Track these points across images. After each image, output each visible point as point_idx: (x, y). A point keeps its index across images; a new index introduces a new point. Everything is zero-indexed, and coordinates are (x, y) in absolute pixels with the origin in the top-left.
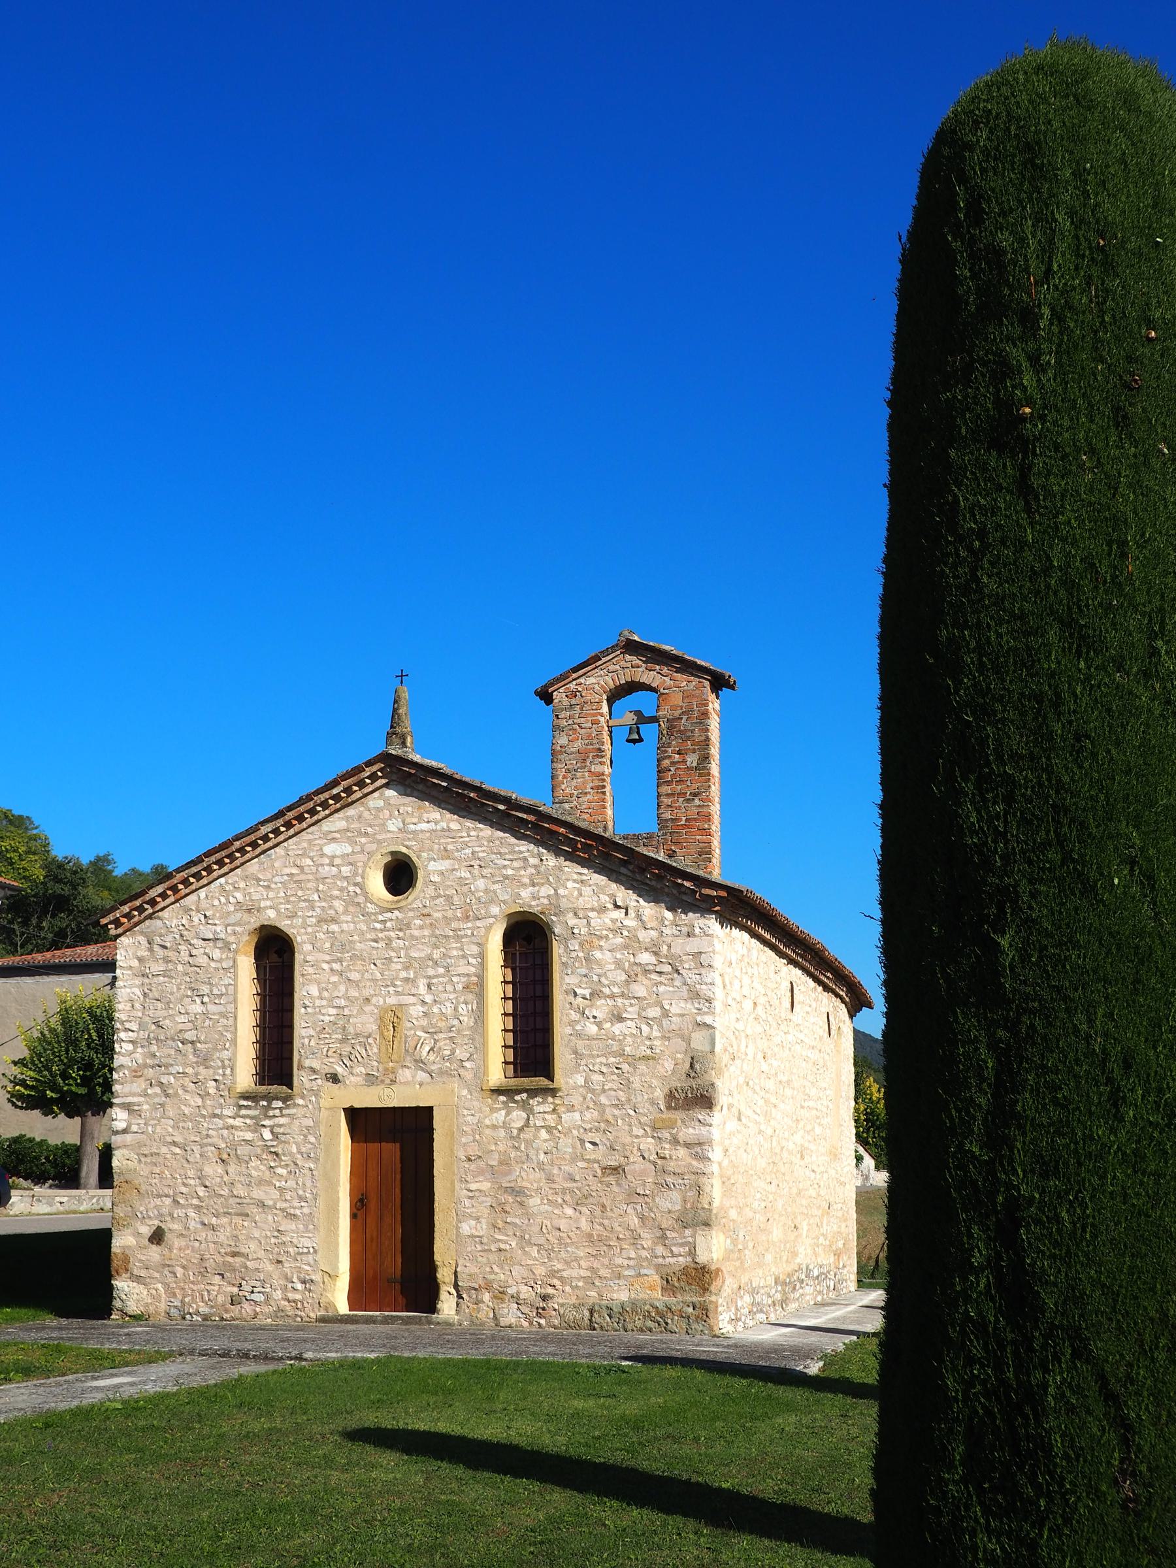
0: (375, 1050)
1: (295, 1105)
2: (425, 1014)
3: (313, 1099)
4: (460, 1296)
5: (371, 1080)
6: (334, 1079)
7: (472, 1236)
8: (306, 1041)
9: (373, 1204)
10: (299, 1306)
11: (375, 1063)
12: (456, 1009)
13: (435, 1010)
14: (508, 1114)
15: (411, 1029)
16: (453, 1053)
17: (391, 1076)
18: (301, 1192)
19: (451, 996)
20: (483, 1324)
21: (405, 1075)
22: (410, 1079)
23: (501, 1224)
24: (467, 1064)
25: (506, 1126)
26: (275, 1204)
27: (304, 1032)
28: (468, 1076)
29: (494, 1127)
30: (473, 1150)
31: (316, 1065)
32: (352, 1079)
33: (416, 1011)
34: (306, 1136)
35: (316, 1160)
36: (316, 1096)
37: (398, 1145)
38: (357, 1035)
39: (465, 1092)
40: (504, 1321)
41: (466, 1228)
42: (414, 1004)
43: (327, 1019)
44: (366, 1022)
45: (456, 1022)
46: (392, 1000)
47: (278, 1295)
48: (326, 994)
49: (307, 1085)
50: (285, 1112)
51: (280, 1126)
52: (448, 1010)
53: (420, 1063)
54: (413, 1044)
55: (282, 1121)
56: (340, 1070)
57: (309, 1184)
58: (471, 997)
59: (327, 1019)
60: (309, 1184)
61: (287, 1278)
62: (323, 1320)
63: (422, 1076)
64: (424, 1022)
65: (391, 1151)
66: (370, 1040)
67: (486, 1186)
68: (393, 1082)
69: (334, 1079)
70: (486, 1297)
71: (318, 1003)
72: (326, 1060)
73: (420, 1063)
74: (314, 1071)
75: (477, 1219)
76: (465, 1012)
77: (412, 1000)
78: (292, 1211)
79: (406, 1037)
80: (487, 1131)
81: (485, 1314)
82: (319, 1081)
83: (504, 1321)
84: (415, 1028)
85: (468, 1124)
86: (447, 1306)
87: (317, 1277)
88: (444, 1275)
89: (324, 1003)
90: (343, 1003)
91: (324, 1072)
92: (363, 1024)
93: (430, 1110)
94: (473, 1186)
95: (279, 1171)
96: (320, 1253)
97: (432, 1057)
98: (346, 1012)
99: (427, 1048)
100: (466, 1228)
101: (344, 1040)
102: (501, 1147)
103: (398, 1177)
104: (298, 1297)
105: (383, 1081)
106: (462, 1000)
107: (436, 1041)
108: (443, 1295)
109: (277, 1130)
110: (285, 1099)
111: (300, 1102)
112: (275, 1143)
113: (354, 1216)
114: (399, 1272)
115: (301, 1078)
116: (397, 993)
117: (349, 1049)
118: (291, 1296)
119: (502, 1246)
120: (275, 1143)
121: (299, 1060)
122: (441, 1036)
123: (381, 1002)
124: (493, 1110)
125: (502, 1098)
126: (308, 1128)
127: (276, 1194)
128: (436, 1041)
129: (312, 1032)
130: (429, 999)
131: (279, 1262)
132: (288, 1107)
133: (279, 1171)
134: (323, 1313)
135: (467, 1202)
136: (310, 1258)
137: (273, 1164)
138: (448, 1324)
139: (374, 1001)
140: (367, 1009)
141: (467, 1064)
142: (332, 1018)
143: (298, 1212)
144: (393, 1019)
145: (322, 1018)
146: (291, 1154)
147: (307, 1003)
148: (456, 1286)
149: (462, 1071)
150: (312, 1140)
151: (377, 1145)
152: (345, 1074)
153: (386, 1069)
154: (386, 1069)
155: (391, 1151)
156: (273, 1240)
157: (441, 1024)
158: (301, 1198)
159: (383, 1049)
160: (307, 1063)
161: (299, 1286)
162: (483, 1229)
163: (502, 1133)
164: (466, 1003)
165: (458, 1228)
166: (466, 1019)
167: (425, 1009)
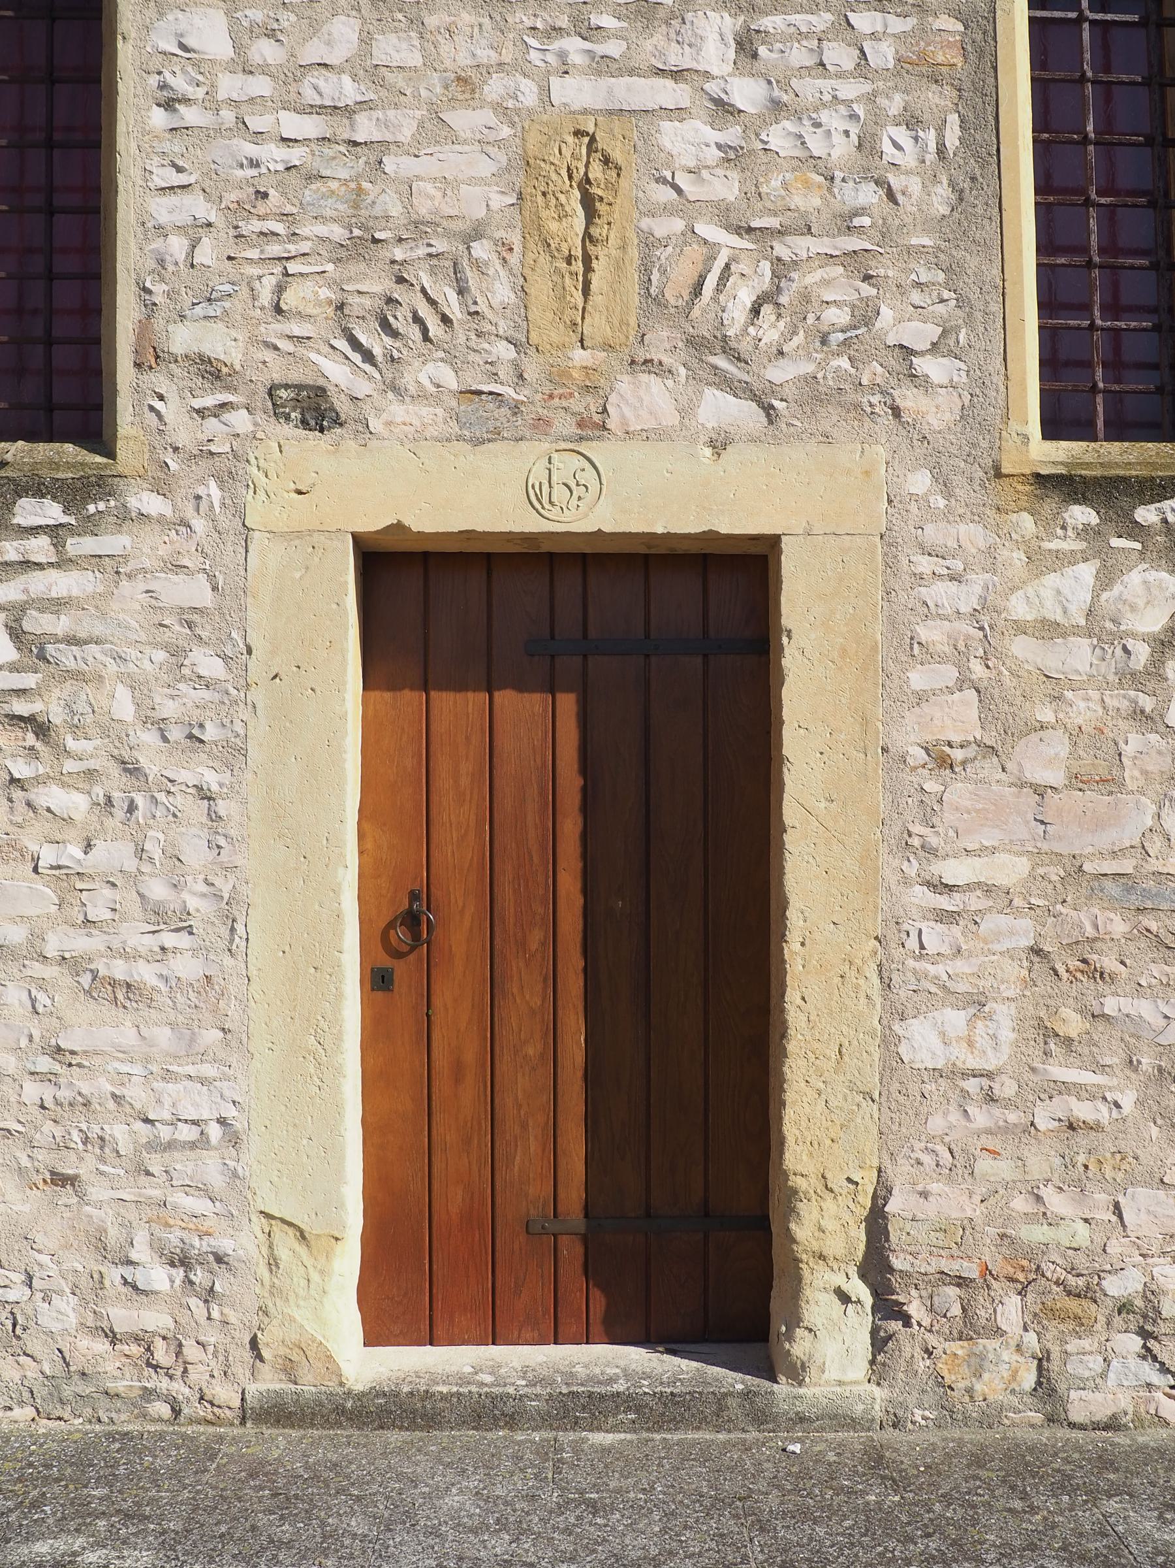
0: (503, 292)
1: (124, 517)
2: (732, 156)
3: (214, 490)
4: (887, 1307)
5: (483, 414)
6: (314, 410)
7: (954, 1073)
8: (177, 246)
9: (460, 929)
10: (162, 1355)
11: (505, 352)
12: (867, 145)
13: (778, 137)
14: (1106, 579)
15: (668, 210)
16: (865, 315)
17: (577, 404)
18: (158, 890)
19: (850, 90)
20: (990, 1418)
21: (642, 400)
22: (671, 418)
23: (1073, 1024)
24: (933, 368)
25: (1099, 627)
26: (37, 936)
27: (163, 210)
28: (935, 411)
29: (1049, 630)
30: (959, 719)
31: (222, 344)
32: (398, 411)
33: (690, 140)
34: (177, 653)
35: (234, 753)
36: (226, 479)
37: (568, 703)
38: (419, 227)
39: (920, 482)
40: (1083, 1405)
41: (926, 1041)
42: (678, 113)
43: (274, 155)
44: (461, 177)
45: (869, 195)
46: (578, 93)
47: (62, 1315)
48: (265, 51)
49: (184, 431)
50: (77, 546)
51: (57, 605)
52: (835, 144)
53: (710, 348)
54: (683, 272)
55: (61, 583)
56: (338, 373)
57: (196, 854)
58: (936, 98)
59: (274, 155)
60: (196, 854)
61: (100, 1246)
62: (276, 1413)
63: (720, 408)
64: (726, 187)
65: (537, 726)
66: (481, 250)
67: (1010, 870)
68: (594, 427)
69: (314, 410)
70: (1011, 1312)
71: (229, 85)
72: (274, 330)
73: (710, 348)
74: (211, 371)
75: (978, 1002)
76: (908, 159)
77: (669, 93)
78: (119, 970)
79: (649, 242)
80: (1022, 648)
81: (1002, 1376)
82: (240, 420)
83: (1083, 1405)
84: (684, 205)
85: (929, 613)
86: (831, 1341)
87: (243, 1243)
88: (822, 1229)
89: (261, 86)
90: (348, 91)
91: (264, 379)
92: (446, 184)
93: (773, 542)
94: (954, 871)
95: (53, 797)
96: (254, 1146)
97: (770, 330)
98: (365, 128)
99: (746, 297)
100: (926, 1041)
101: (363, 244)
102: (1083, 710)
103: (571, 827)
104: (156, 1319)
105: (541, 424)
106: (895, 105)
107: (781, 269)
108: (817, 1306)
109: (37, 623)
110: (76, 493)
111: (153, 504)
112: (29, 680)
113: (378, 980)
114: (574, 1195)
115: (140, 402)
116: (602, 66)
117: (379, 284)
118: (122, 1317)
119: (1083, 1111)
120: (29, 680)
121: (144, 329)
122: (804, 246)
123: (529, 95)
124: (1041, 562)
125: (1082, 515)
126: (189, 617)
127: (41, 898)
128: (781, 269)
129: (202, 209)
130: (747, 93)
131: (60, 1180)
132: (90, 526)
133: (53, 797)
134: (267, 1383)
135: (935, 937)
136: (211, 1168)
137: (21, 770)
138: (842, 1420)
139: (495, 88)
140: (463, 120)
141: (933, 368)
142: (296, 155)
143: (146, 974)
144: (585, 175)
145: (251, 150)
146: (108, 728)
147: (179, 84)
148: (876, 1266)
149: (909, 399)
150: (209, 665)
151: (476, 700)
152: (363, 388)
153: (558, 377)
154: (558, 377)
155: (537, 726)
156: (32, 1091)
157: (807, 201)
158: (158, 915)
159: (541, 289)
160: (182, 339)
161: (159, 1277)
162: (998, 1042)
163: (1079, 656)
164: (912, 121)
165: (889, 1041)
166: (915, 185)
167: (732, 135)
